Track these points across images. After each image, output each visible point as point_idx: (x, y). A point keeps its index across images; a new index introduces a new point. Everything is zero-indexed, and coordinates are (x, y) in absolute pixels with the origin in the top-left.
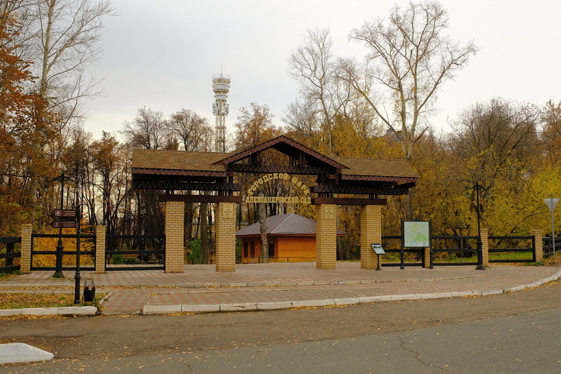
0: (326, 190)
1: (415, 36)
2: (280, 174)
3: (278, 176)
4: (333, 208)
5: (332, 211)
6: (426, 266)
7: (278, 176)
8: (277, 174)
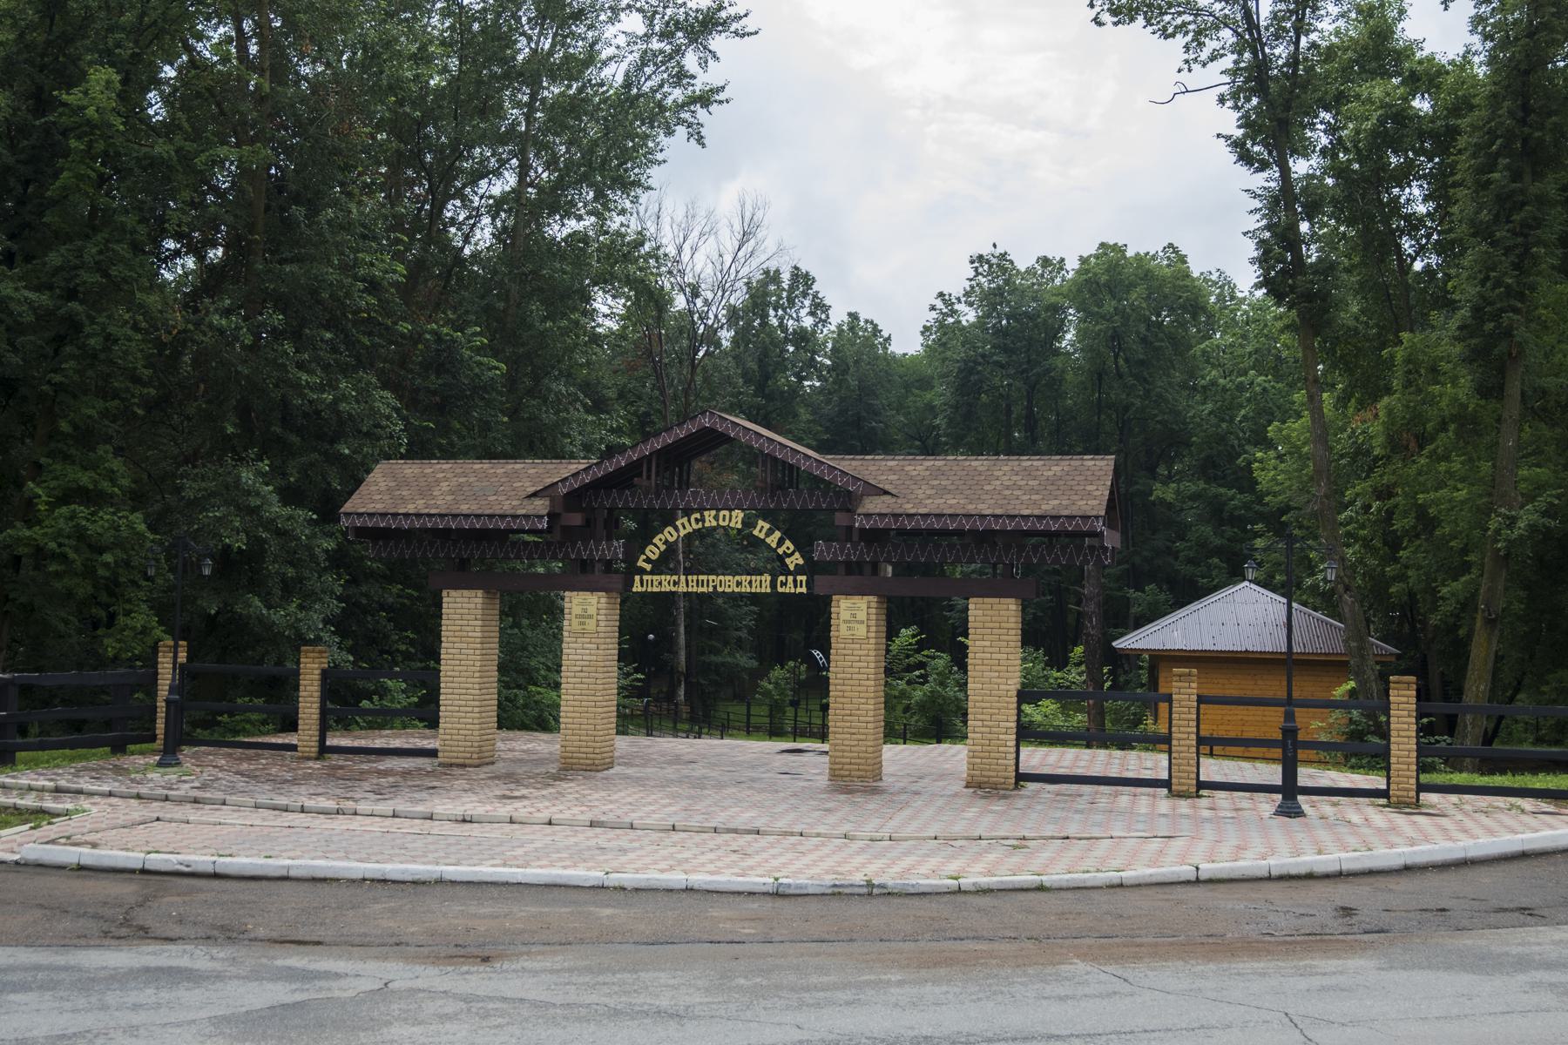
0: (848, 555)
1: (1262, 18)
2: (722, 513)
3: (716, 518)
4: (864, 606)
5: (862, 616)
6: (1025, 751)
7: (716, 518)
8: (713, 513)
